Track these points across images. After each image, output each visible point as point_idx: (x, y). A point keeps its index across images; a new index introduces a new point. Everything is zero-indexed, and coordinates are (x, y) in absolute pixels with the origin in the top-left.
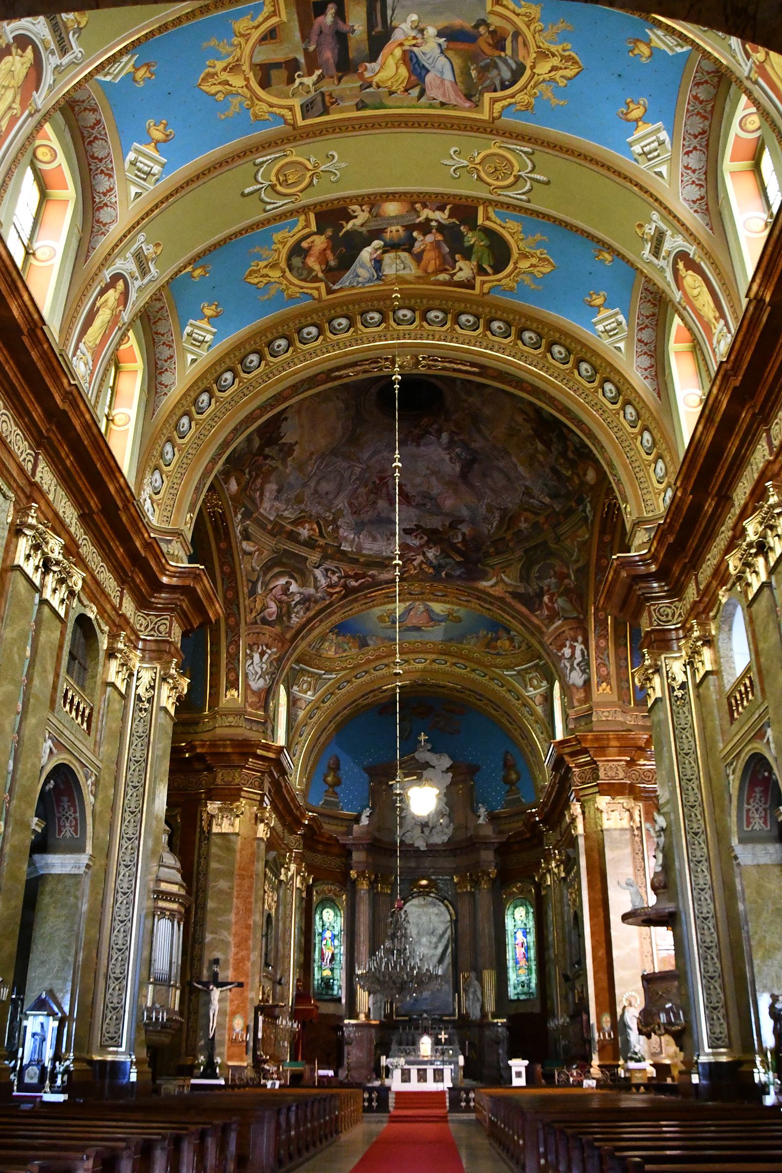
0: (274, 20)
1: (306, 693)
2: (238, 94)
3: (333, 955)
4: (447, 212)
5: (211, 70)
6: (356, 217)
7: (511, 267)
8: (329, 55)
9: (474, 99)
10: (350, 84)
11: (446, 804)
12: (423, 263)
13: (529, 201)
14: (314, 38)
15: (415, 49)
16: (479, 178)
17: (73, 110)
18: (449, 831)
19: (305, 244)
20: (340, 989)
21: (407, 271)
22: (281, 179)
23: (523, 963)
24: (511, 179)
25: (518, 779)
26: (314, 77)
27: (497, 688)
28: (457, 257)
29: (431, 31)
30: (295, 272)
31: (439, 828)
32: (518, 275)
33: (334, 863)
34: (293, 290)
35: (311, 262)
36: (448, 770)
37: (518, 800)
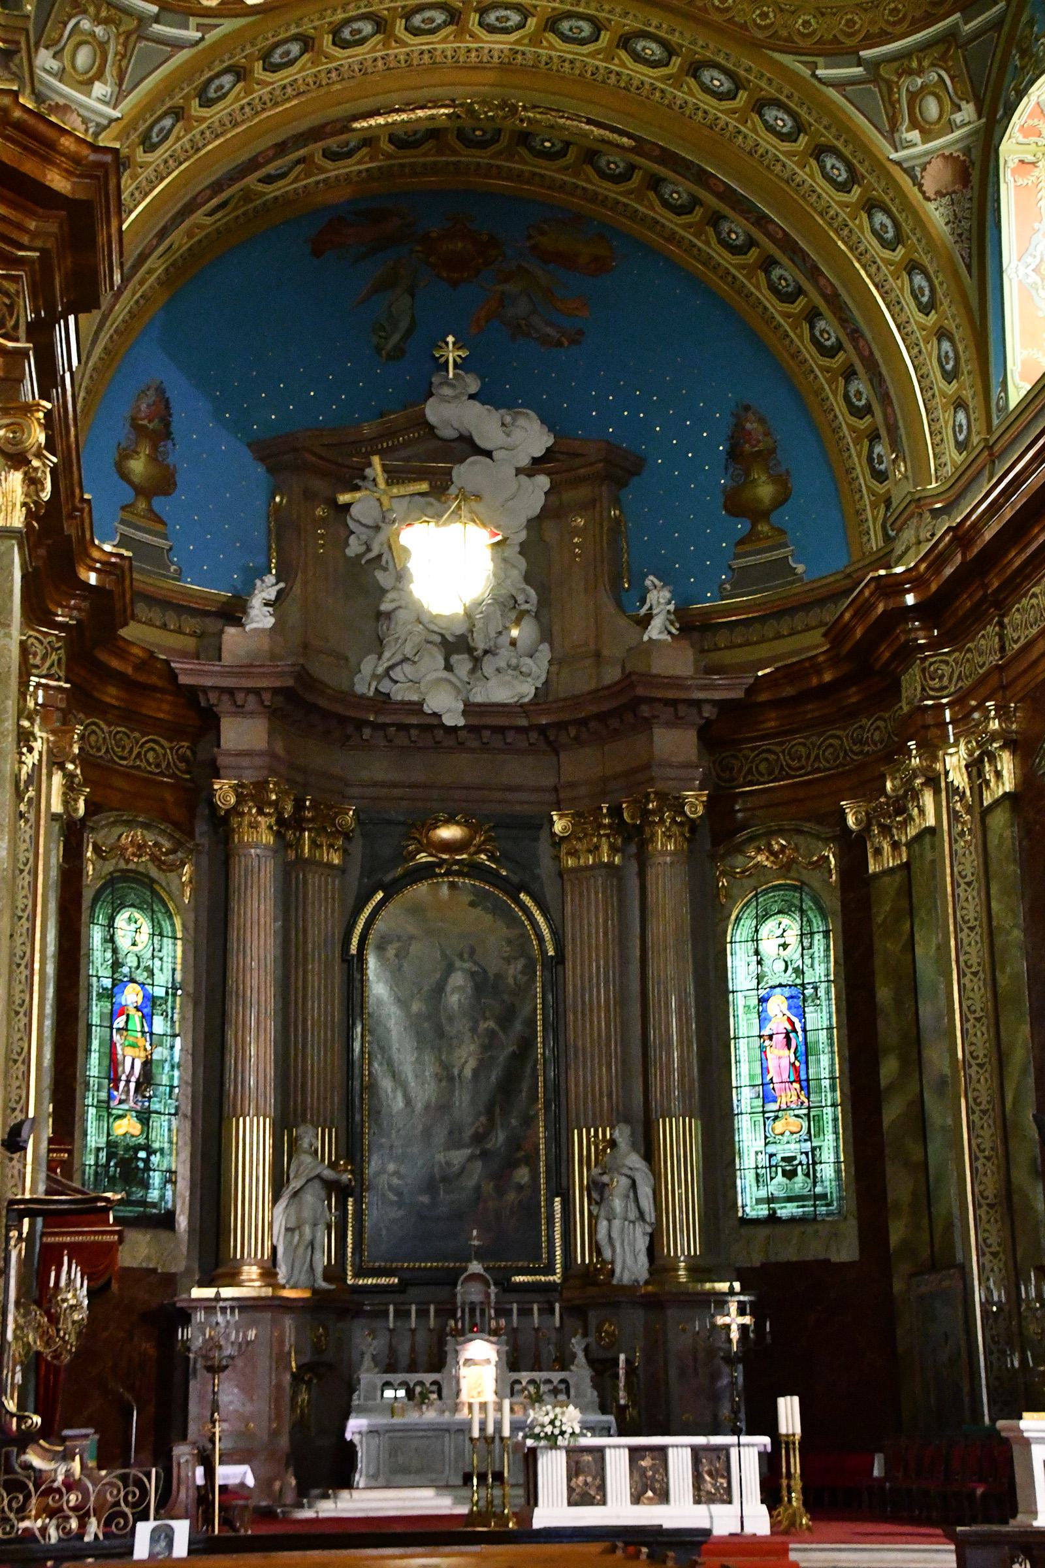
1: (86, 85)
3: (147, 1063)
11: (528, 578)
18: (539, 667)
20: (169, 1182)
23: (788, 1095)
25: (782, 499)
27: (768, 142)
31: (505, 655)
33: (154, 754)
36: (537, 465)
37: (781, 568)
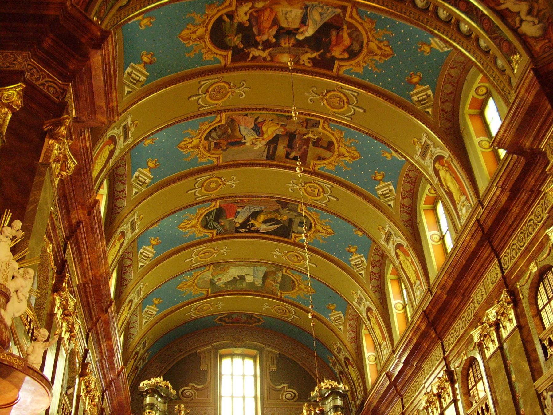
0: (317, 162)
2: (345, 145)
4: (251, 56)
5: (351, 159)
6: (309, 59)
7: (210, 27)
8: (298, 142)
9: (230, 120)
10: (291, 128)
12: (272, 18)
13: (200, 82)
14: (302, 150)
15: (257, 137)
16: (229, 84)
17: (415, 180)
19: (346, 56)
21: (285, 10)
22: (342, 103)
24: (210, 90)
26: (307, 136)
28: (247, 24)
29: (248, 144)
30: (361, 40)
32: (205, 21)
34: (368, 26)
35: (347, 41)
